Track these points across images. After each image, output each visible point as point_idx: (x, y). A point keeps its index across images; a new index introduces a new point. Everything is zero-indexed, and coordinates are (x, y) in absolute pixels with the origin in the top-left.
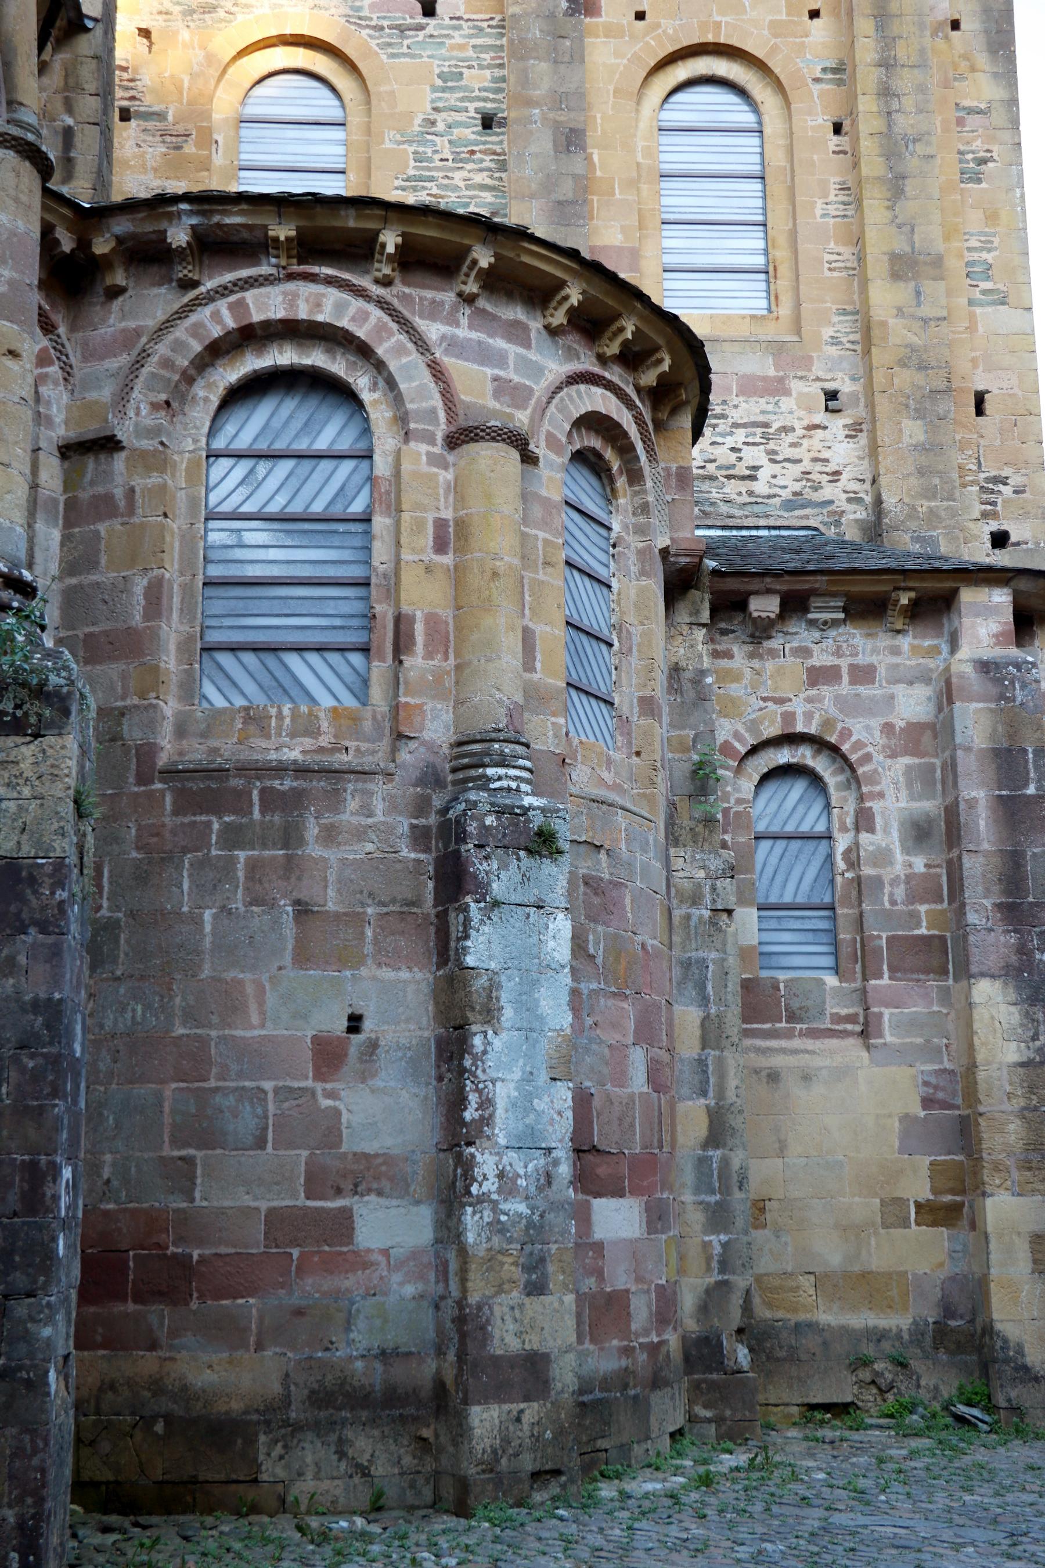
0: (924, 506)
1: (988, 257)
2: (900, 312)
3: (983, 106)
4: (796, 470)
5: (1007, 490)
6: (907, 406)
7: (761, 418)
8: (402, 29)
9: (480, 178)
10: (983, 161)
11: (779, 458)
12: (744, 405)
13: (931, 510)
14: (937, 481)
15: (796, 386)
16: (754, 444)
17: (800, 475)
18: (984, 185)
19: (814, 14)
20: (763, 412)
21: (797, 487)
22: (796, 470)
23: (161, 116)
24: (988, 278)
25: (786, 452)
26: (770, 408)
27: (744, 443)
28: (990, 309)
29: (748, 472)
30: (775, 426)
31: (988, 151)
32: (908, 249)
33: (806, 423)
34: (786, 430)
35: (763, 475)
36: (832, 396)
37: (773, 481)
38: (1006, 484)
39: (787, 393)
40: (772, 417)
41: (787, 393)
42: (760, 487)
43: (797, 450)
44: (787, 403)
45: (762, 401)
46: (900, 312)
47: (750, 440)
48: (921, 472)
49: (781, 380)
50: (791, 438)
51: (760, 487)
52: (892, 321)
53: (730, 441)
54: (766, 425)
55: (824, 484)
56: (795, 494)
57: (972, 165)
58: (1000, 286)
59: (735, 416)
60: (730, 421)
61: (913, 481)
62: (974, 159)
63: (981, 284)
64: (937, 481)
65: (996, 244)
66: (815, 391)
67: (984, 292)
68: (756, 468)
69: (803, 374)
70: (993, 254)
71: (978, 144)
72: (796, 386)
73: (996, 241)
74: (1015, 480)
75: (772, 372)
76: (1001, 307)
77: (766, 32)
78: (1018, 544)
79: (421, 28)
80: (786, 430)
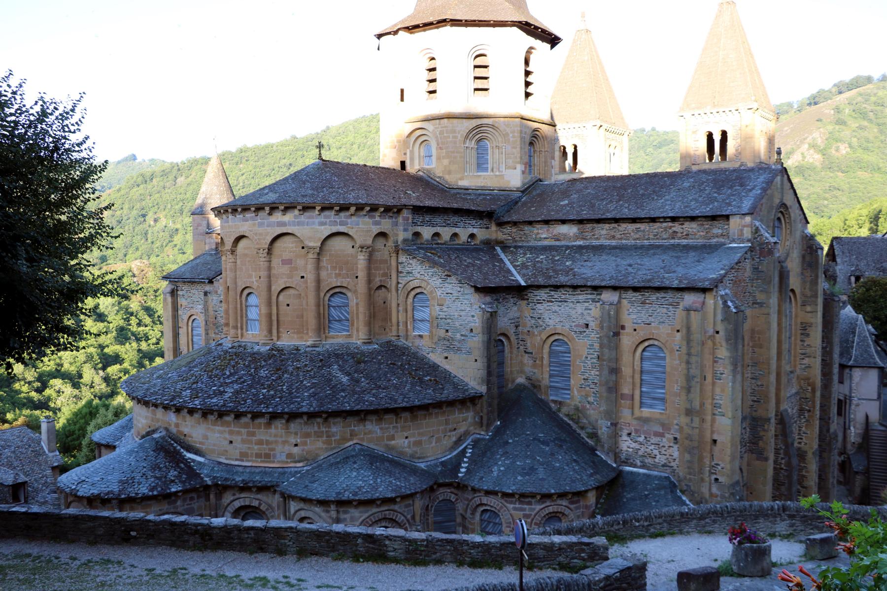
0: (688, 477)
1: (721, 402)
2: (687, 425)
5: (719, 468)
9: (597, 373)
15: (667, 435)
19: (678, 331)
23: (532, 353)
25: (664, 452)
35: (658, 457)
36: (675, 439)
42: (657, 460)
44: (664, 440)
46: (687, 425)
48: (689, 468)
51: (657, 460)
59: (652, 441)
61: (687, 470)
66: (671, 437)
71: (721, 369)
72: (667, 435)
74: (722, 465)
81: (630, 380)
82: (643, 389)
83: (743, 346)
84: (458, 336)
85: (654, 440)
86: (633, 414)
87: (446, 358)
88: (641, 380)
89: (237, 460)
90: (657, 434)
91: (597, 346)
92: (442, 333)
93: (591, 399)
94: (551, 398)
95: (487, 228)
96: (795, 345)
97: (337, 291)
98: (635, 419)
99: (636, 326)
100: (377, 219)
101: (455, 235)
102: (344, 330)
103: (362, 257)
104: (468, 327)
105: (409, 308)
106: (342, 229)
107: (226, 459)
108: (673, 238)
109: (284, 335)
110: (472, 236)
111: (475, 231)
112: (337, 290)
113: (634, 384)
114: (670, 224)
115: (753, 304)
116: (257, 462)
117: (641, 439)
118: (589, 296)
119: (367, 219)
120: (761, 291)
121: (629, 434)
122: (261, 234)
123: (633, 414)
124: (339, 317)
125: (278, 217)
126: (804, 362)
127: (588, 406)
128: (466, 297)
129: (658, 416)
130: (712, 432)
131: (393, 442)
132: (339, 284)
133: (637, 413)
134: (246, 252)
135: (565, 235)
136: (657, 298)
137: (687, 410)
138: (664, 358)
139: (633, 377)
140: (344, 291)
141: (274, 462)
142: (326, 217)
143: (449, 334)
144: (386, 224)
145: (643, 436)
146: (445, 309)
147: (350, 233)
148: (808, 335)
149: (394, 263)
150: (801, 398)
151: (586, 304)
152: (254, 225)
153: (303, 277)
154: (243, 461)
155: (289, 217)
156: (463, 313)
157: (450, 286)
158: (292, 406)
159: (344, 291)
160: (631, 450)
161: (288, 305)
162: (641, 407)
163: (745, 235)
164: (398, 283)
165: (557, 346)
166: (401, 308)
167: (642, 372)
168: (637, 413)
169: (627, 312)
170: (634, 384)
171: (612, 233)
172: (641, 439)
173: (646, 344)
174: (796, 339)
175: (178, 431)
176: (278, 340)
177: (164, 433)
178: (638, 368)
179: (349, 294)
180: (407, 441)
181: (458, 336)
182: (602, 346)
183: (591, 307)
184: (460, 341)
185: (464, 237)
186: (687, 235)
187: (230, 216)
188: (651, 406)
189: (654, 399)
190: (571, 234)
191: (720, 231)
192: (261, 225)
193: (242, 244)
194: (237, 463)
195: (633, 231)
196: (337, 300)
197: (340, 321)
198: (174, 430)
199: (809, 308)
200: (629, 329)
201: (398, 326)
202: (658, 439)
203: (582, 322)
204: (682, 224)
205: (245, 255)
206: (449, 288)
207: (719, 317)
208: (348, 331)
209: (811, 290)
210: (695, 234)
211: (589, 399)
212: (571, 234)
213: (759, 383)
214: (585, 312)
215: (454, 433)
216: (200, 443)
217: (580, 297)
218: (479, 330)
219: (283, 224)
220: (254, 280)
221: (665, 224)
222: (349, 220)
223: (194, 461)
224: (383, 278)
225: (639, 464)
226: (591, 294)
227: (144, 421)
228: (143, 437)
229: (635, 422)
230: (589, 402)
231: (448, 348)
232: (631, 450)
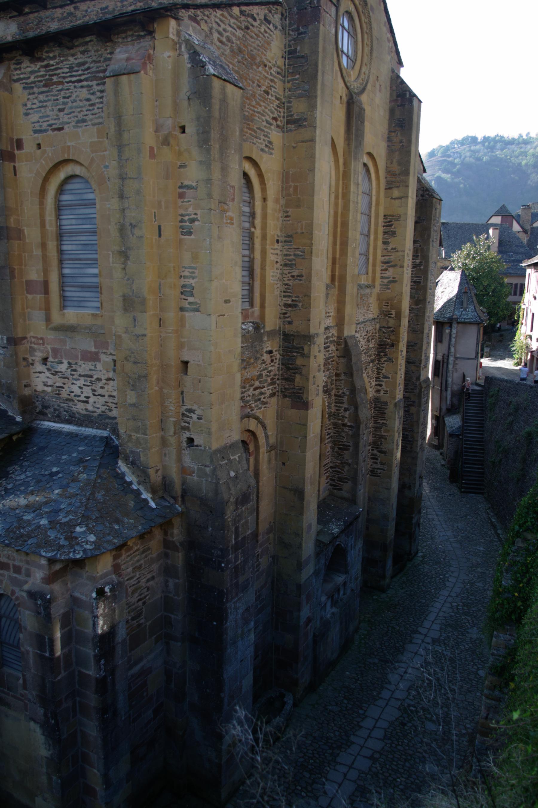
1: (192, 282)
3: (194, 184)
6: (129, 383)
7: (89, 373)
10: (192, 221)
11: (96, 393)
12: (83, 366)
13: (138, 438)
14: (140, 424)
15: (103, 357)
16: (87, 386)
17: (104, 403)
18: (193, 237)
20: (90, 370)
21: (103, 409)
22: (102, 400)
24: (192, 295)
25: (100, 391)
26: (93, 368)
27: (84, 385)
28: (192, 314)
29: (85, 399)
30: (95, 377)
31: (196, 214)
32: (131, 294)
33: (106, 377)
34: (99, 380)
35: (91, 400)
37: (94, 405)
38: (194, 414)
39: (99, 360)
40: (94, 373)
41: (99, 360)
42: (90, 407)
43: (103, 390)
44: (99, 366)
45: (90, 363)
47: (86, 383)
49: (97, 353)
50: (100, 384)
52: (124, 335)
54: (91, 377)
55: (113, 408)
56: (103, 412)
57: (187, 224)
58: (197, 300)
59: (81, 371)
60: (78, 373)
62: (189, 219)
63: (188, 298)
64: (140, 424)
65: (196, 275)
67: (190, 303)
68: (88, 397)
69: (104, 351)
70: (196, 280)
73: (197, 271)
75: (93, 349)
76: (197, 313)
77: (88, 150)
78: (197, 446)
80: (99, 380)
81: (37, 252)
82: (66, 271)
83: (265, 199)
85: (84, 367)
86: (48, 319)
88: (61, 252)
96: (375, 248)
98: (56, 329)
113: (45, 258)
115: (288, 122)
117: (63, 367)
120: (300, 96)
121: (45, 360)
123: (48, 319)
126: (388, 274)
129: (89, 321)
130: (181, 346)
133: (57, 318)
136: (71, 68)
139: (44, 246)
145: (65, 362)
148: (394, 233)
160: (49, 389)
162: (63, 307)
167: (60, 236)
168: (57, 318)
169: (22, 110)
170: (45, 258)
173: (62, 175)
174: (376, 240)
178: (51, 228)
188: (80, 304)
189: (84, 287)
199: (396, 193)
200: (29, 147)
207: (185, 88)
209: (399, 164)
213: (295, 274)
229: (50, 336)
232: (49, 389)
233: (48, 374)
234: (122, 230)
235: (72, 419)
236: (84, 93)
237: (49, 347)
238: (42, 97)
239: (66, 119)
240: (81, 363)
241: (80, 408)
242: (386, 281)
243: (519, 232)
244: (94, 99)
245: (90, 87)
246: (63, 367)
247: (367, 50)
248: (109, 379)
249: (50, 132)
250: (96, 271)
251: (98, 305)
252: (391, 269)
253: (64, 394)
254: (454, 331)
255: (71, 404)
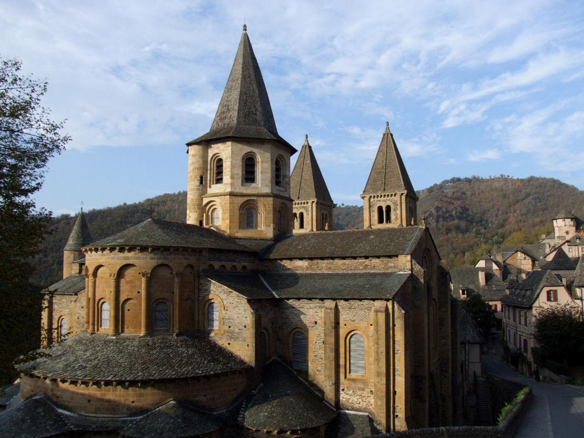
2: (378, 382)
4: (366, 403)
5: (399, 408)
8: (312, 327)
15: (366, 389)
19: (371, 325)
22: (366, 403)
23: (282, 340)
25: (364, 400)
36: (371, 391)
39: (365, 390)
41: (365, 390)
42: (360, 406)
44: (365, 392)
50: (365, 398)
53: (356, 398)
59: (357, 393)
66: (369, 390)
73: (399, 365)
74: (400, 407)
75: (363, 387)
79: (315, 326)
84: (237, 330)
85: (359, 392)
87: (229, 344)
89: (93, 413)
90: (360, 389)
91: (322, 335)
92: (226, 328)
93: (319, 368)
94: (294, 368)
95: (253, 262)
97: (162, 301)
99: (346, 323)
100: (187, 256)
101: (234, 266)
102: (166, 326)
103: (177, 280)
104: (243, 325)
105: (206, 312)
106: (165, 262)
107: (86, 412)
108: (366, 269)
109: (126, 330)
110: (244, 267)
111: (246, 264)
112: (161, 301)
114: (364, 260)
116: (106, 414)
118: (317, 305)
119: (180, 256)
122: (113, 265)
123: (346, 377)
124: (162, 318)
125: (126, 254)
127: (317, 373)
128: (242, 305)
129: (360, 378)
131: (196, 399)
132: (162, 297)
134: (103, 275)
135: (301, 267)
137: (378, 372)
138: (363, 342)
140: (165, 301)
141: (118, 414)
142: (155, 254)
143: (231, 328)
144: (192, 260)
145: (352, 391)
146: (229, 313)
147: (170, 265)
149: (196, 284)
150: (441, 363)
151: (316, 309)
152: (109, 258)
153: (139, 292)
154: (96, 413)
155: (132, 254)
156: (240, 316)
157: (232, 298)
158: (131, 376)
159: (165, 301)
161: (129, 310)
163: (408, 267)
164: (199, 296)
165: (298, 335)
166: (200, 313)
171: (329, 266)
172: (351, 392)
173: (352, 333)
175: (53, 395)
176: (122, 333)
177: (42, 396)
179: (168, 304)
180: (205, 398)
181: (237, 330)
182: (325, 335)
183: (318, 311)
184: (237, 333)
185: (239, 268)
186: (374, 267)
187: (94, 252)
189: (358, 367)
190: (305, 267)
191: (393, 265)
192: (113, 258)
193: (101, 270)
194: (93, 415)
195: (341, 264)
196: (161, 307)
197: (161, 320)
198: (50, 393)
199: (443, 310)
201: (199, 323)
202: (361, 392)
203: (313, 320)
204: (371, 261)
205: (103, 278)
206: (231, 300)
208: (166, 327)
210: (379, 267)
211: (318, 368)
212: (305, 267)
213: (419, 355)
214: (315, 314)
215: (235, 392)
216: (68, 402)
217: (312, 305)
218: (250, 325)
219: (127, 258)
220: (107, 293)
221: (361, 260)
222: (169, 257)
223: (62, 414)
224: (190, 293)
225: (350, 408)
226: (318, 303)
227: (29, 388)
228: (27, 399)
230: (318, 370)
231: (231, 338)
232: (344, 400)
233: (344, 394)
234: (377, 353)
235: (353, 409)
236: (363, 312)
237: (345, 386)
238: (348, 311)
239: (356, 318)
240: (357, 391)
241: (357, 406)
242: (441, 344)
243: (497, 270)
244: (366, 315)
245: (365, 311)
246: (351, 392)
247: (430, 264)
248: (368, 396)
249: (350, 321)
250: (364, 362)
251: (364, 372)
252: (443, 340)
253: (350, 401)
254: (467, 347)
255: (353, 404)
